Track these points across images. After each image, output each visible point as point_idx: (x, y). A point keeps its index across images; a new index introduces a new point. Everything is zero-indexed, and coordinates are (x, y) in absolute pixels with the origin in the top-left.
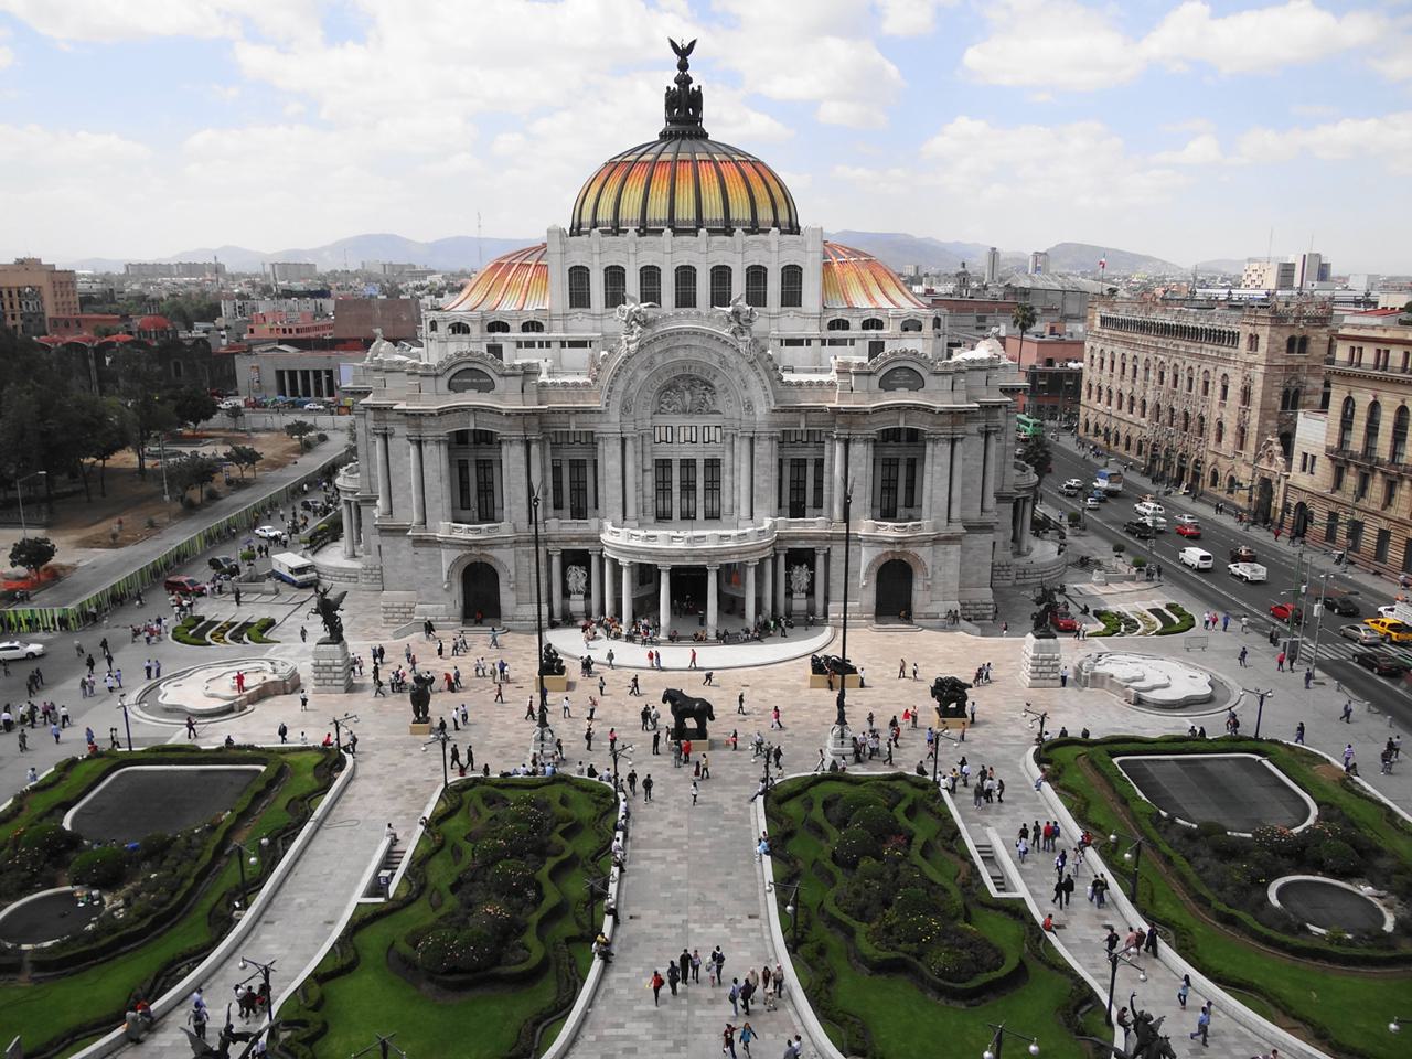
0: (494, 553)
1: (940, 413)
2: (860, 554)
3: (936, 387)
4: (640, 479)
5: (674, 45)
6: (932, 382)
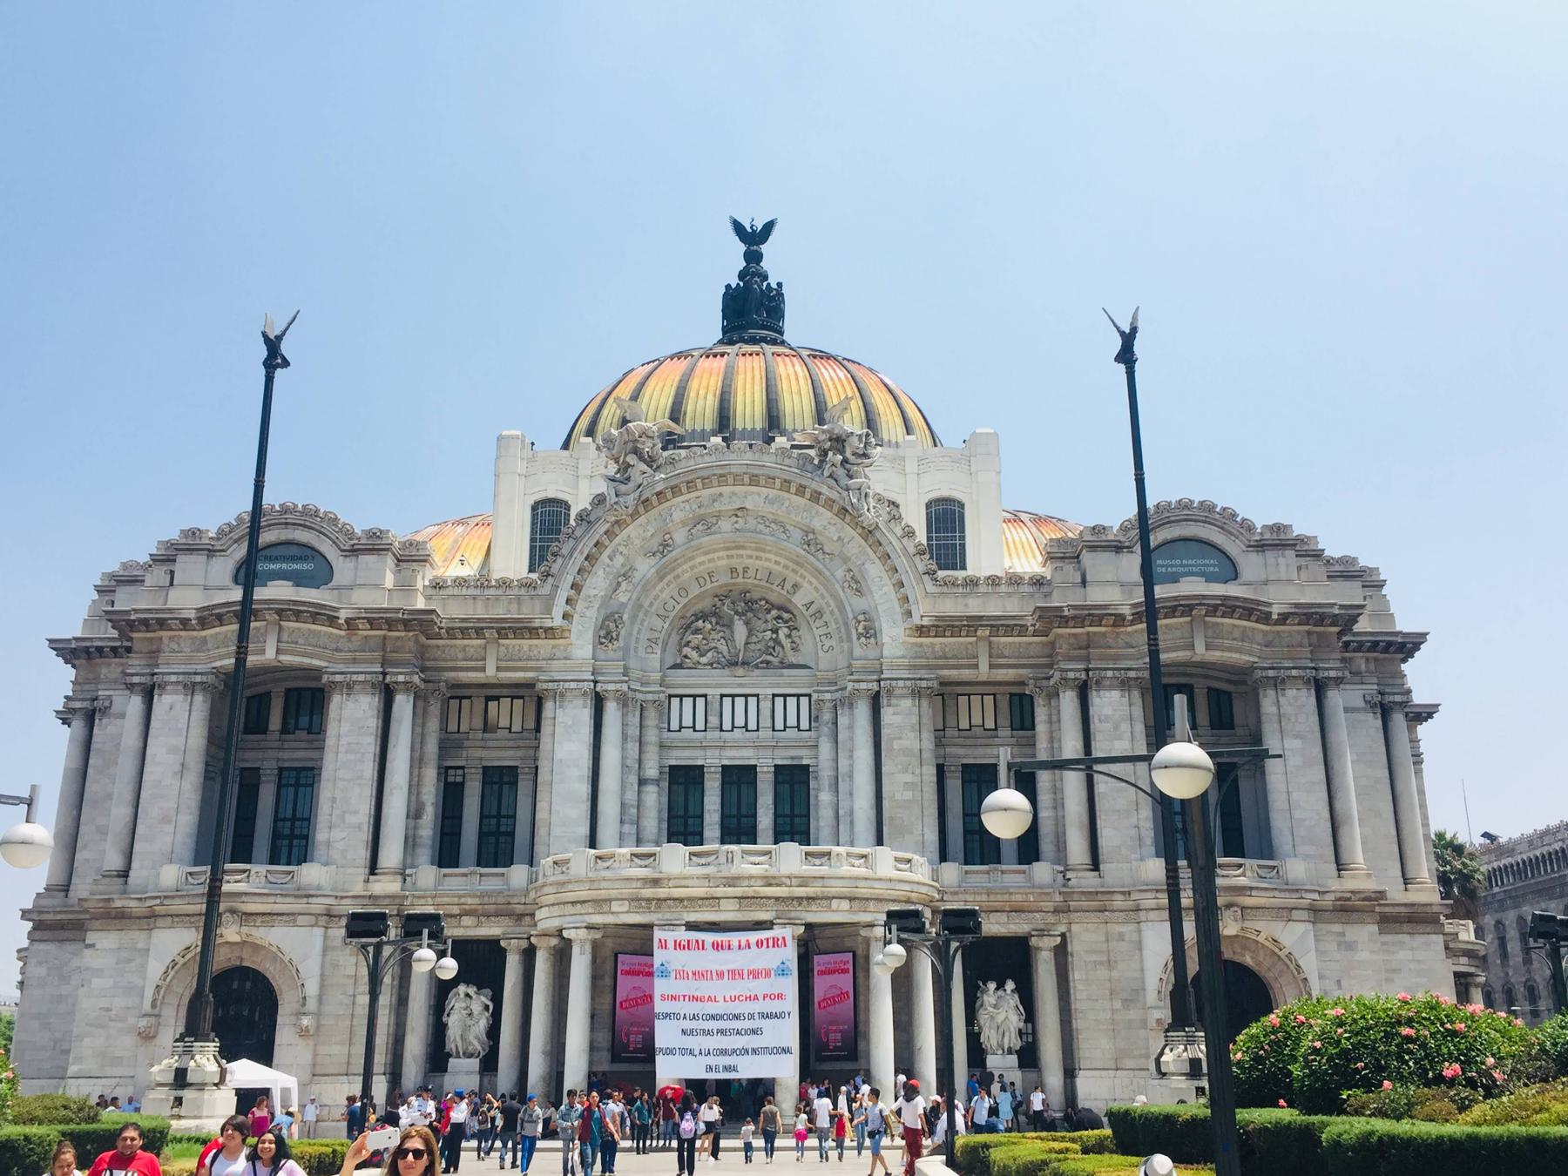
0: (273, 935)
1: (1284, 618)
2: (1139, 946)
3: (1263, 577)
4: (631, 796)
5: (738, 227)
6: (1251, 565)
